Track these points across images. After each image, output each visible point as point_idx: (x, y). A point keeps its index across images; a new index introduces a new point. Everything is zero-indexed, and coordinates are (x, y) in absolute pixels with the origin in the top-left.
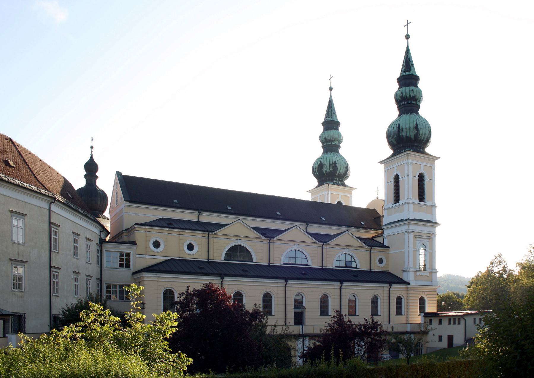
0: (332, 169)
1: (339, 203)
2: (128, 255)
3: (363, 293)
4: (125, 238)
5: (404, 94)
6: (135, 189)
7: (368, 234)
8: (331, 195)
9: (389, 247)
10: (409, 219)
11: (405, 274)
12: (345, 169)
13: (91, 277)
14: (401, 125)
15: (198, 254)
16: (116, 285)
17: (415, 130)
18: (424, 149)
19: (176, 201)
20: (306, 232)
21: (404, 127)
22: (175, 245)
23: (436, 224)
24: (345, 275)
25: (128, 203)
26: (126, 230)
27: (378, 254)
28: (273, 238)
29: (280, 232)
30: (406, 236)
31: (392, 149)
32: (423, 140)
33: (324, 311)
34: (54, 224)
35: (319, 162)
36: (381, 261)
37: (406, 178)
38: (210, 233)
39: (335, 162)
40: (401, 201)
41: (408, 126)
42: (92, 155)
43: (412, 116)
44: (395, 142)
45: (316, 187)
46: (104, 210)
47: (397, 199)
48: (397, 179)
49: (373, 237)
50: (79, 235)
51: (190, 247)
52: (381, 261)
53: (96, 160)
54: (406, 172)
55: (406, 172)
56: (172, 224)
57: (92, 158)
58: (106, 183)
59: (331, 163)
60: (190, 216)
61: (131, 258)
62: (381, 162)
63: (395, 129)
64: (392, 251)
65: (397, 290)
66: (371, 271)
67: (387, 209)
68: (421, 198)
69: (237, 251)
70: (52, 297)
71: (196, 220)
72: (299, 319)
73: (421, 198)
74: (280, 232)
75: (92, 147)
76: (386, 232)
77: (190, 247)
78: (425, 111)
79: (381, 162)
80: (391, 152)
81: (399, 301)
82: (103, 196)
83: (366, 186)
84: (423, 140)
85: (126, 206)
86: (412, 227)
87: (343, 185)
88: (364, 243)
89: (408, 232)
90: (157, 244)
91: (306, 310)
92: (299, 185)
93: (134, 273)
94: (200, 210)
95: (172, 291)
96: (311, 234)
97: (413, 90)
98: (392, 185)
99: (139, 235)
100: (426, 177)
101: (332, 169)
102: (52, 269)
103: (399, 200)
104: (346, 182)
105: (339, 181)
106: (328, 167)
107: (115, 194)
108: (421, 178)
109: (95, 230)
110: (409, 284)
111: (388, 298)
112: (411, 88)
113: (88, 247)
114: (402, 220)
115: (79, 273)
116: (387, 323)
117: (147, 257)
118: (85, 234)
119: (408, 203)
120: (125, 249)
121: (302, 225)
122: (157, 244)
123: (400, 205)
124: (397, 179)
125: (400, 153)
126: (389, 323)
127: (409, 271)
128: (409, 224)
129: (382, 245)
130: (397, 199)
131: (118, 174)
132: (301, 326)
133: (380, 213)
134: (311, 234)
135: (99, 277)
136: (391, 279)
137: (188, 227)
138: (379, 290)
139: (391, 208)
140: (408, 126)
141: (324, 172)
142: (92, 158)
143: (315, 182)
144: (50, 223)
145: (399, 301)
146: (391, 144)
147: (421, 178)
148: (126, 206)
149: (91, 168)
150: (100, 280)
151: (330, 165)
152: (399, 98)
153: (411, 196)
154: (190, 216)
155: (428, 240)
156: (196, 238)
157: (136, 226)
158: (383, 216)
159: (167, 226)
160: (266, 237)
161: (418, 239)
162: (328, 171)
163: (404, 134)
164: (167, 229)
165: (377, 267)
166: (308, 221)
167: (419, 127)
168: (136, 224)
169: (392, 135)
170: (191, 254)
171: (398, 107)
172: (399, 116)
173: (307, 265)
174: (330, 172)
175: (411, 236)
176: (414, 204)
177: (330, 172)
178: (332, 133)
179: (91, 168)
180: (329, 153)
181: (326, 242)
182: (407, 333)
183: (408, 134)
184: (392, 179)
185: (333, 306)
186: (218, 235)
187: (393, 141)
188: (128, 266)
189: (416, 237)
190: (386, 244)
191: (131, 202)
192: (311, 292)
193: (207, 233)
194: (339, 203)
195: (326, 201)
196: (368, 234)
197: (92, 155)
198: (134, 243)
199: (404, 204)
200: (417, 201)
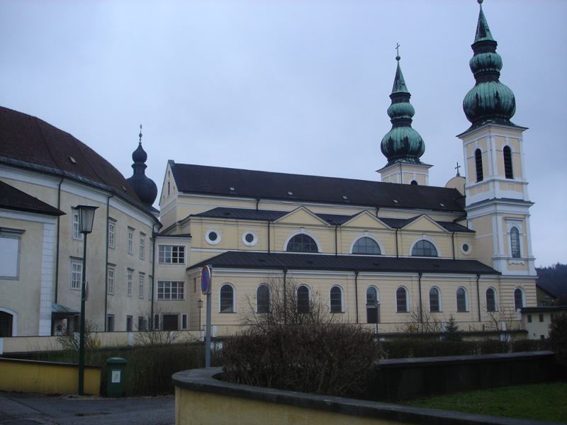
0: (403, 146)
1: (414, 183)
2: (182, 249)
3: (448, 286)
4: (178, 232)
5: (481, 61)
6: (190, 178)
7: (448, 218)
8: (404, 175)
9: (474, 232)
10: (495, 199)
11: (495, 262)
12: (418, 144)
13: (144, 274)
14: (479, 95)
15: (258, 246)
16: (169, 282)
17: (496, 100)
18: (508, 119)
19: (232, 189)
20: (377, 217)
21: (483, 97)
22: (232, 237)
23: (530, 204)
24: (424, 263)
25: (182, 194)
26: (179, 222)
27: (461, 240)
28: (340, 225)
29: (348, 218)
30: (494, 218)
31: (471, 121)
32: (506, 109)
33: (402, 306)
34: (112, 219)
35: (388, 138)
36: (466, 248)
37: (489, 152)
38: (271, 222)
39: (407, 137)
40: (485, 179)
41: (487, 96)
42: (140, 143)
43: (491, 84)
44: (473, 113)
45: (386, 166)
46: (152, 202)
47: (480, 177)
48: (478, 153)
49: (455, 221)
50: (133, 229)
51: (249, 238)
52: (466, 248)
53: (145, 149)
54: (489, 145)
55: (489, 145)
56: (229, 214)
57: (140, 146)
58: (156, 172)
59: (402, 139)
60: (247, 204)
61: (186, 252)
62: (459, 136)
63: (473, 98)
64: (478, 236)
65: (486, 283)
66: (454, 260)
67: (470, 188)
68: (509, 174)
69: (303, 242)
70: (108, 296)
71: (255, 209)
72: (373, 316)
73: (509, 174)
74: (348, 218)
75: (141, 135)
76: (470, 215)
77: (249, 238)
78: (508, 78)
79: (459, 136)
80: (470, 124)
81: (490, 293)
82: (152, 186)
83: (444, 163)
84: (506, 109)
85: (179, 196)
86: (500, 208)
87: (418, 162)
88: (445, 227)
89: (496, 213)
90: (213, 236)
91: (381, 306)
92: (368, 165)
93: (188, 269)
94: (258, 197)
95: (231, 287)
96: (382, 219)
97: (490, 56)
98: (474, 161)
99: (194, 228)
100: (513, 150)
101: (403, 146)
102: (109, 266)
103: (482, 177)
104: (422, 159)
105: (412, 158)
106: (399, 143)
107: (167, 184)
108: (507, 151)
109: (148, 222)
110: (500, 274)
111: (476, 291)
112: (488, 54)
113: (142, 241)
114: (488, 200)
115: (133, 270)
116: (478, 320)
117: (203, 250)
118: (139, 228)
119: (494, 181)
120: (178, 243)
121: (372, 211)
122: (213, 236)
123: (484, 183)
124: (478, 153)
125: (480, 125)
126: (480, 321)
127: (499, 259)
128: (496, 204)
129: (467, 230)
130: (480, 177)
131: (171, 162)
132: (375, 325)
133: (462, 192)
134: (382, 219)
135: (151, 274)
136: (477, 268)
137: (252, 217)
138: (466, 281)
139: (473, 187)
140: (487, 96)
141: (395, 149)
142: (140, 146)
143: (384, 161)
144: (108, 218)
145: (490, 293)
146: (470, 117)
147: (507, 151)
148: (179, 196)
149: (140, 157)
150: (152, 277)
151: (401, 141)
152: (474, 65)
153: (496, 173)
154: (247, 204)
155: (520, 222)
156: (258, 230)
157: (191, 218)
158: (465, 196)
159: (224, 216)
160: (332, 224)
161: (508, 221)
162: (399, 147)
163: (483, 104)
164: (224, 219)
165: (461, 255)
166: (378, 205)
167: (500, 95)
168: (191, 215)
169: (470, 105)
170: (250, 246)
171: (475, 76)
172: (477, 84)
173: (380, 254)
174: (402, 151)
175: (500, 218)
176: (500, 181)
177: (402, 151)
178: (402, 105)
179: (140, 157)
180: (399, 128)
181: (400, 228)
182: (499, 333)
183: (488, 105)
184: (473, 155)
185: (411, 302)
186: (280, 224)
187: (471, 112)
188: (182, 261)
189: (505, 219)
190: (470, 228)
191: (185, 191)
192: (387, 286)
193: (267, 222)
194: (414, 183)
195: (399, 182)
196: (448, 218)
197: (140, 143)
198: (189, 236)
199: (488, 182)
200: (504, 178)
